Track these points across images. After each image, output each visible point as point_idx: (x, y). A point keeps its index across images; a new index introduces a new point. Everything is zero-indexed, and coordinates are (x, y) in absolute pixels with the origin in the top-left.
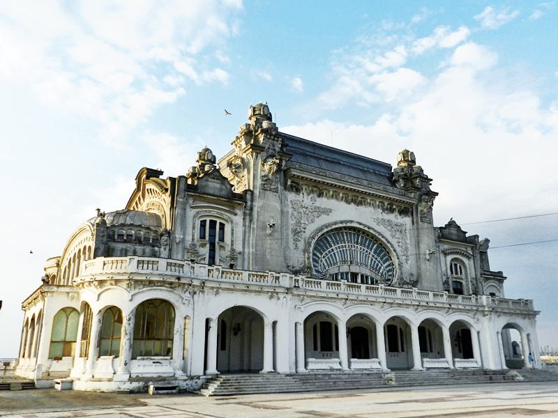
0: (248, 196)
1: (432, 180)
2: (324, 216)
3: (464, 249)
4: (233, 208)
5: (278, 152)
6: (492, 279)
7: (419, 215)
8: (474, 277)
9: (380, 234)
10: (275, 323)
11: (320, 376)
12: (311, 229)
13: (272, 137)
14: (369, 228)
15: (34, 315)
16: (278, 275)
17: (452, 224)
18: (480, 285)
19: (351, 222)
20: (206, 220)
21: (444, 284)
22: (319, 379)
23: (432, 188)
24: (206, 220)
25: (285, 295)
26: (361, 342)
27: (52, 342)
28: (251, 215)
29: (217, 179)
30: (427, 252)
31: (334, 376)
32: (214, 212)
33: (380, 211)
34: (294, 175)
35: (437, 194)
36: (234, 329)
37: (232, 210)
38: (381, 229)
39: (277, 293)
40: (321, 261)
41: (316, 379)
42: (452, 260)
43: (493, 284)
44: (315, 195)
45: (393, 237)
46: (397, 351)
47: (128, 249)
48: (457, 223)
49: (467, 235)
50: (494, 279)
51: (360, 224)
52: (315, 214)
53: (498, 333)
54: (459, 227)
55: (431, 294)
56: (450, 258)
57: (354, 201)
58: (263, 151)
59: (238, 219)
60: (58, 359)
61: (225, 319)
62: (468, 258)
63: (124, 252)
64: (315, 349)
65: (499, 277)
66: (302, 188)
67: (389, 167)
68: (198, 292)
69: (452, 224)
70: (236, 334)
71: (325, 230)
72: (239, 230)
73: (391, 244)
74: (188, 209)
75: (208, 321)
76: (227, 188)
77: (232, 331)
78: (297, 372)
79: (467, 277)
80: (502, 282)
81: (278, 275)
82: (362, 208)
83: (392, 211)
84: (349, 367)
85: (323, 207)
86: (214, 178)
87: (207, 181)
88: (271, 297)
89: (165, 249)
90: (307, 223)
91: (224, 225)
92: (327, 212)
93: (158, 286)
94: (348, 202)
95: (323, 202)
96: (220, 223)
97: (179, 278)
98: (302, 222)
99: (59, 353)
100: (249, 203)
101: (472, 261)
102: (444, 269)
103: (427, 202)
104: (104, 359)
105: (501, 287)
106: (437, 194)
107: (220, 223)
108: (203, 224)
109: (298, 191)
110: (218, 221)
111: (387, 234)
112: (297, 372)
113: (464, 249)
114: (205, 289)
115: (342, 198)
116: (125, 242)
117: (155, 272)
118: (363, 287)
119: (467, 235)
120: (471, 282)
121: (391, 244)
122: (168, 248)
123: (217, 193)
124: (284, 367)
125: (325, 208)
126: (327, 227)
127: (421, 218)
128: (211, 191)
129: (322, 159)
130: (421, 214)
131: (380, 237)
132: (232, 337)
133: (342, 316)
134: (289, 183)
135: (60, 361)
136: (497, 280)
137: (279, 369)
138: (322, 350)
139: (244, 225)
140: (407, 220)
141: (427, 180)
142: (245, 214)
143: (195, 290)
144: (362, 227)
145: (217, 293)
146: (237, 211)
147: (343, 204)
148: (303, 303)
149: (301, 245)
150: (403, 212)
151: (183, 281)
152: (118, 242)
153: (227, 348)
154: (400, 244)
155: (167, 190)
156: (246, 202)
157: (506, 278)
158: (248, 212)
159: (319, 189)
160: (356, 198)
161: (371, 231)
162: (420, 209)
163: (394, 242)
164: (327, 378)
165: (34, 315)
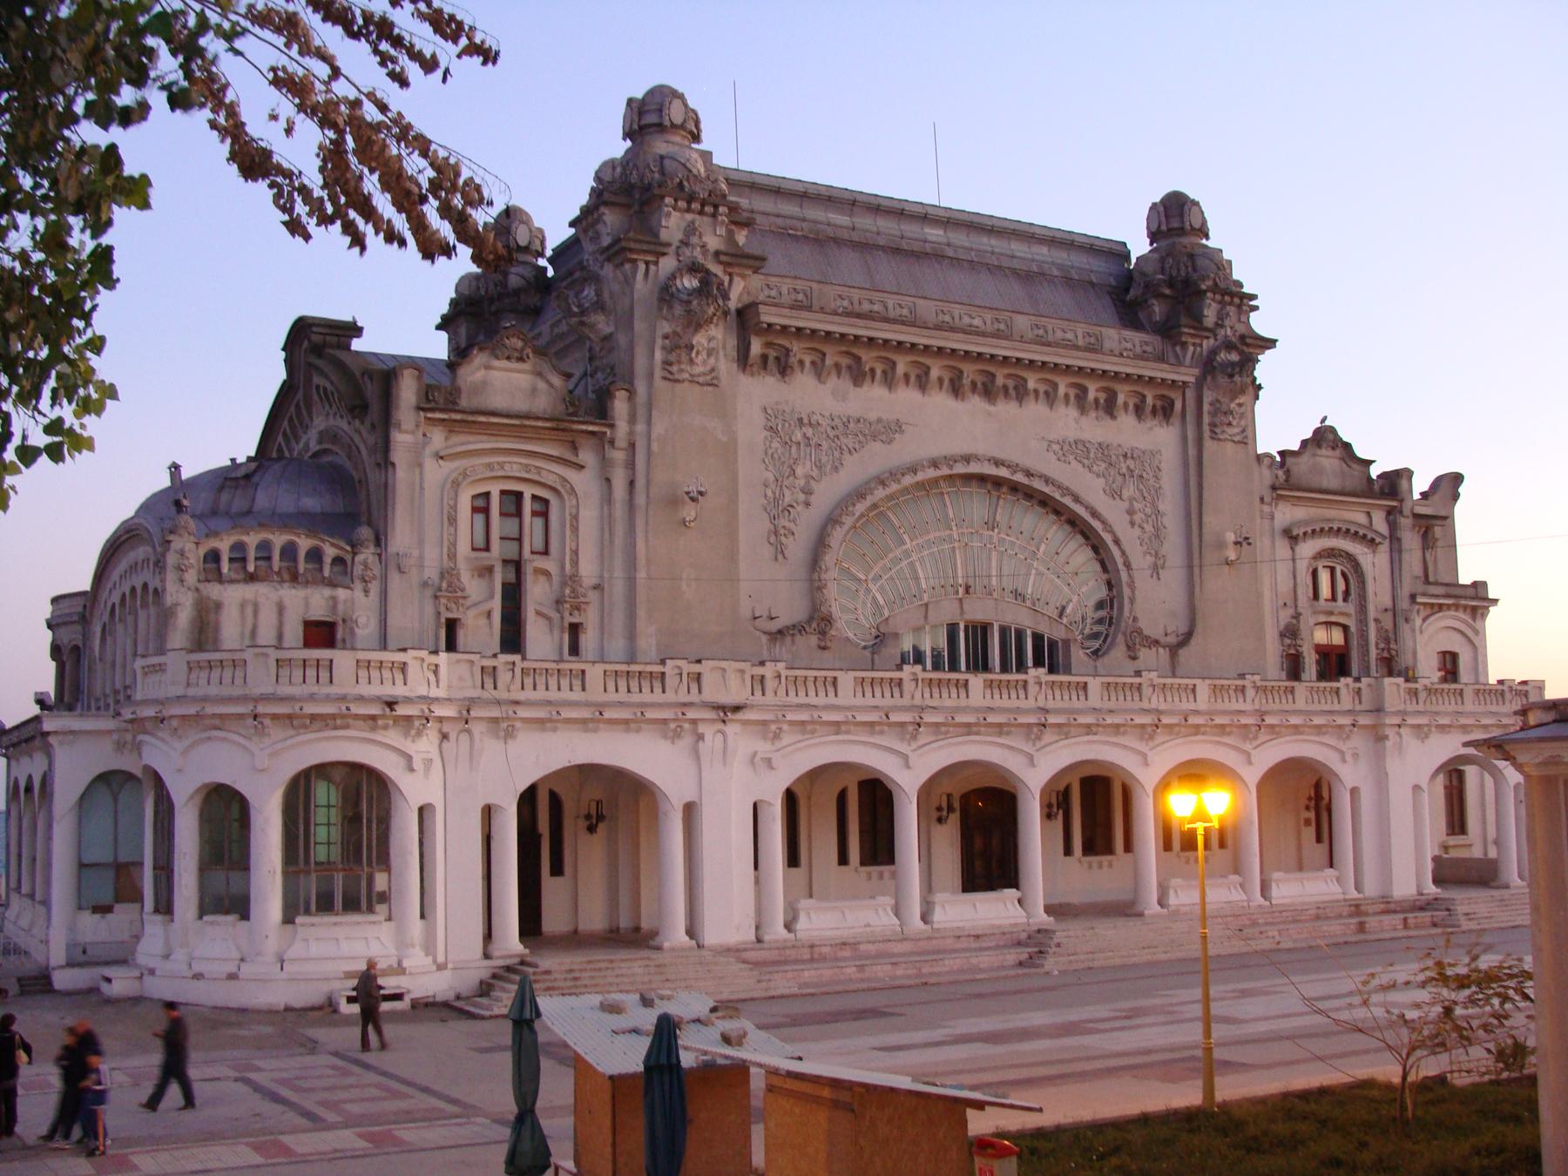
0: (620, 405)
1: (1254, 297)
2: (876, 447)
3: (1361, 518)
4: (574, 448)
5: (717, 254)
6: (1449, 607)
7: (1206, 419)
8: (1389, 604)
9: (1067, 491)
10: (690, 810)
11: (825, 950)
13: (695, 206)
14: (1029, 474)
15: (30, 777)
16: (696, 668)
17: (1324, 437)
18: (1405, 629)
19: (967, 459)
20: (487, 495)
21: (1282, 635)
22: (823, 958)
23: (1259, 323)
24: (487, 495)
25: (720, 726)
26: (985, 833)
27: (82, 866)
28: (631, 464)
29: (521, 359)
30: (1231, 537)
31: (871, 947)
32: (514, 466)
33: (1072, 412)
34: (770, 325)
35: (1270, 343)
36: (588, 817)
37: (569, 456)
39: (694, 722)
40: (868, 590)
41: (812, 960)
42: (1319, 556)
43: (1457, 624)
44: (845, 383)
45: (1115, 494)
46: (1109, 850)
47: (261, 600)
48: (1340, 434)
49: (1375, 472)
50: (1457, 607)
51: (998, 463)
52: (849, 442)
53: (1417, 788)
54: (1347, 447)
55: (1203, 688)
56: (1307, 549)
57: (988, 391)
58: (664, 254)
60: (103, 909)
61: (556, 789)
62: (1372, 543)
63: (249, 610)
64: (843, 859)
65: (1476, 600)
66: (801, 362)
67: (1118, 252)
68: (453, 736)
69: (1324, 437)
70: (591, 829)
71: (880, 493)
72: (589, 516)
73: (1104, 522)
74: (430, 464)
75: (488, 812)
76: (551, 385)
77: (583, 824)
78: (759, 940)
80: (1484, 616)
81: (696, 668)
82: (1006, 409)
83: (1109, 407)
84: (925, 917)
85: (872, 416)
86: (508, 358)
87: (488, 367)
88: (677, 735)
89: (366, 592)
90: (815, 473)
91: (546, 502)
92: (888, 430)
93: (335, 728)
94: (956, 390)
95: (873, 400)
96: (534, 497)
97: (391, 704)
98: (799, 471)
99: (106, 896)
100: (622, 427)
101: (1384, 548)
102: (1285, 585)
103: (1231, 376)
104: (212, 923)
105: (1480, 633)
106: (1270, 343)
107: (534, 497)
108: (481, 507)
109: (784, 369)
110: (528, 491)
112: (759, 940)
113: (1361, 518)
114: (478, 729)
115: (940, 380)
116: (252, 578)
117: (326, 690)
118: (976, 681)
119: (1375, 472)
120: (1376, 620)
121: (1104, 522)
122: (374, 587)
123: (521, 405)
124: (728, 922)
125: (879, 420)
126: (883, 483)
127: (1213, 425)
128: (498, 401)
129: (882, 248)
130: (1213, 414)
131: (1067, 501)
132: (584, 836)
133: (910, 772)
134: (756, 347)
135: (109, 916)
136: (1465, 607)
137: (713, 935)
138: (863, 863)
139: (608, 499)
140: (1162, 439)
141: (1242, 301)
142: (605, 464)
143: (445, 730)
144: (1003, 472)
145: (509, 734)
146: (587, 456)
147: (940, 401)
148: (778, 744)
149: (798, 548)
151: (401, 710)
152: (232, 581)
153: (568, 869)
154: (1138, 517)
156: (612, 426)
157: (1495, 601)
158: (618, 456)
159: (858, 358)
160: (989, 378)
161: (1038, 484)
162: (1208, 396)
164: (847, 953)
165: (30, 777)
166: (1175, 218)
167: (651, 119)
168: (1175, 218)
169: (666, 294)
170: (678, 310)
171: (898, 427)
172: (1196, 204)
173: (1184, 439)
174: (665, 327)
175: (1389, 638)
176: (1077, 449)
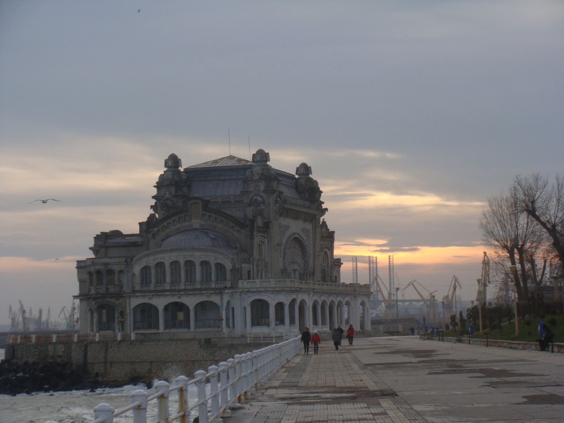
12: (284, 241)
17: (324, 223)
19: (296, 234)
23: (322, 199)
38: (302, 235)
51: (298, 234)
59: (266, 240)
62: (329, 249)
79: (328, 265)
111: (304, 238)
113: (327, 243)
140: (309, 226)
144: (298, 236)
150: (311, 221)
155: (247, 226)
162: (317, 217)
163: (306, 242)
166: (305, 169)
167: (264, 159)
168: (305, 169)
169: (276, 202)
170: (278, 205)
171: (288, 227)
172: (310, 167)
173: (313, 227)
174: (275, 208)
175: (331, 273)
176: (304, 230)
